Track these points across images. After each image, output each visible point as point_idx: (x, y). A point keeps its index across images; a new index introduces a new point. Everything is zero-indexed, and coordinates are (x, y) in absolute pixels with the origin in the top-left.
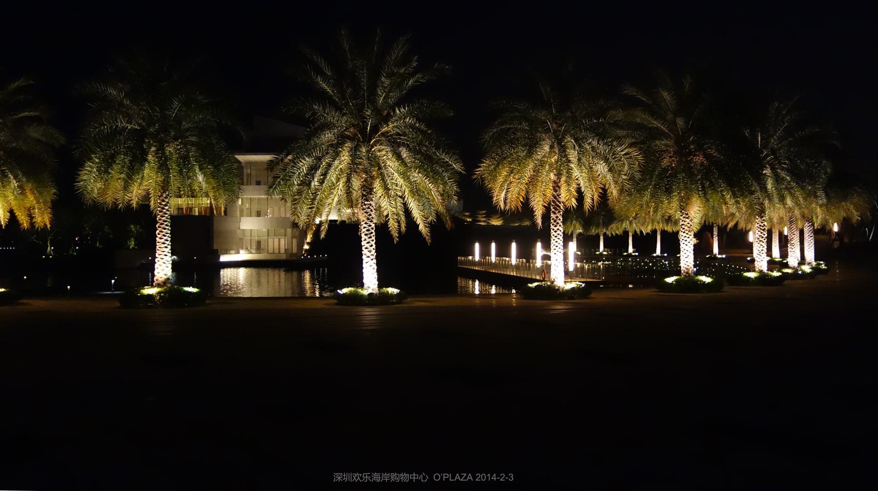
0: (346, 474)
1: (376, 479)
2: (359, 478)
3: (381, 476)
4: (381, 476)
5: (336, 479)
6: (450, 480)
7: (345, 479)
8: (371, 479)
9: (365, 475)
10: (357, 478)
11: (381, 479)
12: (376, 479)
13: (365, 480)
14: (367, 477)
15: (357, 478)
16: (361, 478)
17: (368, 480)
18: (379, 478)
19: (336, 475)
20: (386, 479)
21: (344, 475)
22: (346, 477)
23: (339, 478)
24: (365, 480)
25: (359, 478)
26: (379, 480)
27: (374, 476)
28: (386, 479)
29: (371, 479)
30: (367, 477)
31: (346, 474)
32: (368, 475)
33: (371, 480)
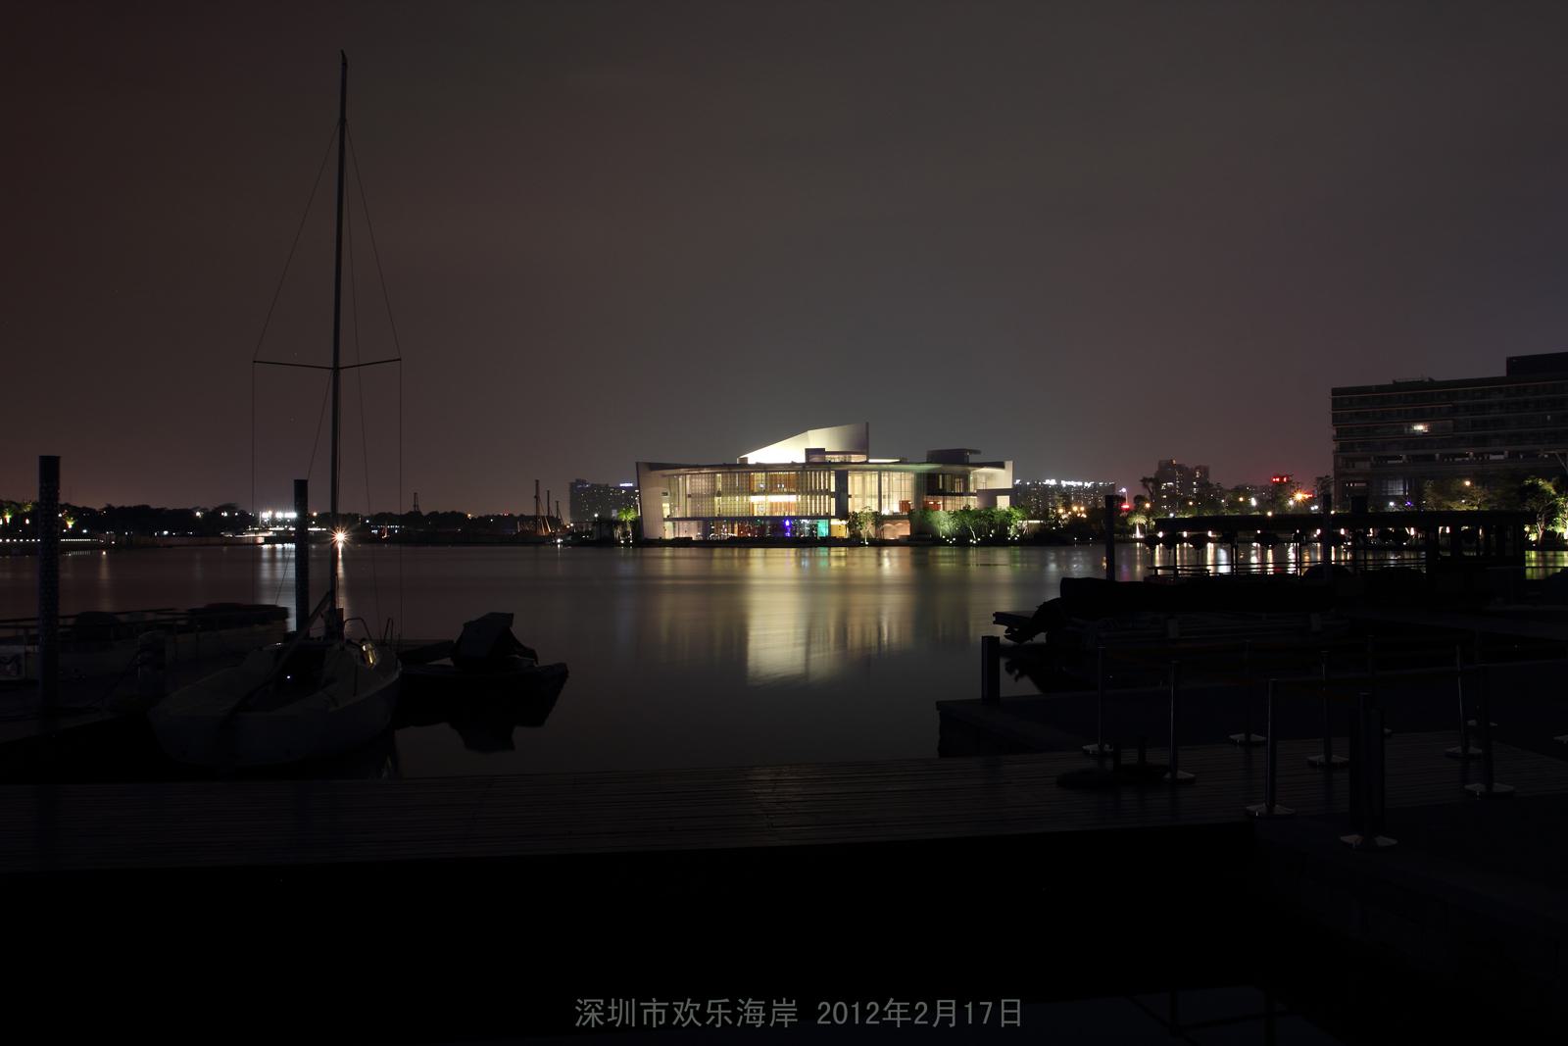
1: (751, 1018)
3: (768, 1009)
4: (768, 1009)
5: (585, 1018)
6: (1003, 1001)
7: (613, 1018)
8: (734, 1016)
9: (715, 1007)
11: (768, 1019)
12: (751, 1018)
16: (702, 1015)
17: (723, 1020)
18: (761, 1014)
19: (582, 1006)
20: (786, 1020)
21: (613, 1007)
26: (761, 1022)
27: (745, 1011)
28: (786, 1020)
29: (734, 1016)
32: (725, 1006)
33: (735, 1021)
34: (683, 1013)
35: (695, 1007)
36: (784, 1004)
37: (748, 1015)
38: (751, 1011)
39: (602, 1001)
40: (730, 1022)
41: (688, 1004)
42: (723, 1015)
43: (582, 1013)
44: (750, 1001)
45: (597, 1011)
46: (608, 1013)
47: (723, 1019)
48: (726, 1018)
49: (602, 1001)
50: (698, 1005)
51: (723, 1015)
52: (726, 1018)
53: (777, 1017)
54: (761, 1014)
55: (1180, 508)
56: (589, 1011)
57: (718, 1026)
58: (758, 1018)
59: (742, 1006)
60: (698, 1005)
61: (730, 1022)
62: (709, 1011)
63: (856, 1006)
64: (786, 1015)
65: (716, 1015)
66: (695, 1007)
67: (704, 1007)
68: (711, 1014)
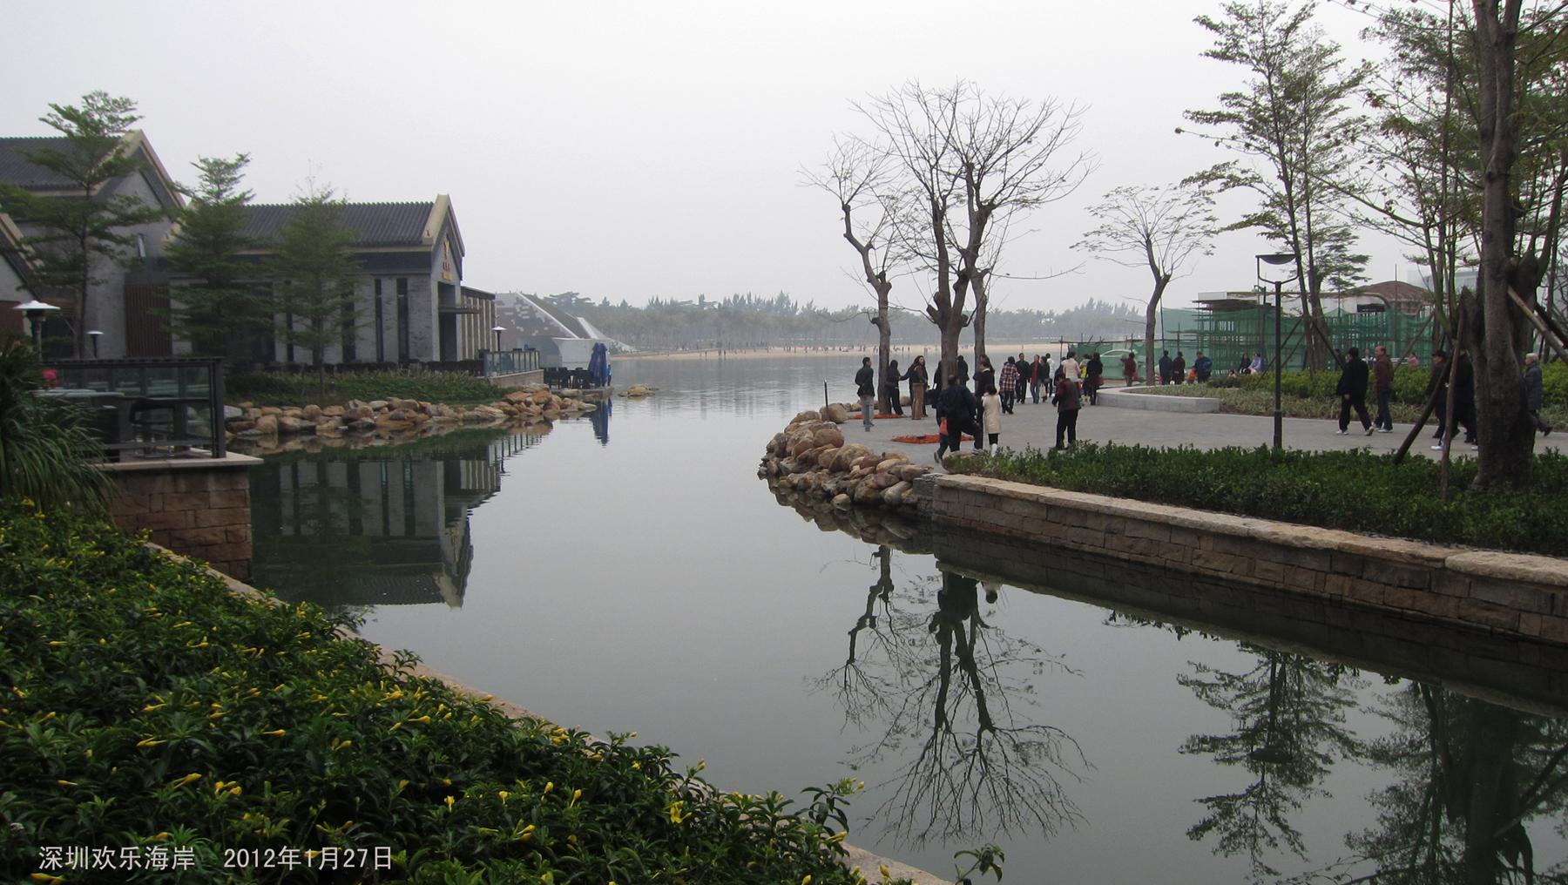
0: (73, 850)
2: (108, 860)
5: (47, 862)
7: (70, 862)
9: (127, 853)
10: (103, 859)
13: (128, 865)
14: (131, 857)
15: (103, 859)
19: (45, 853)
20: (185, 864)
21: (70, 854)
22: (73, 857)
23: (54, 860)
24: (128, 865)
25: (108, 860)
26: (164, 865)
28: (185, 864)
30: (131, 857)
31: (73, 850)
34: (101, 859)
35: (110, 854)
36: (184, 851)
37: (154, 859)
38: (157, 857)
39: (61, 849)
40: (140, 866)
41: (105, 851)
42: (134, 860)
43: (44, 858)
44: (156, 848)
45: (57, 856)
46: (65, 858)
47: (133, 863)
48: (136, 862)
49: (61, 849)
50: (113, 852)
51: (134, 860)
52: (136, 862)
53: (178, 861)
54: (165, 859)
55: (148, 557)
56: (51, 856)
57: (130, 868)
58: (162, 862)
59: (149, 852)
60: (113, 852)
61: (140, 866)
62: (122, 856)
63: (256, 852)
64: (185, 860)
65: (128, 860)
66: (110, 854)
67: (118, 853)
68: (124, 859)
